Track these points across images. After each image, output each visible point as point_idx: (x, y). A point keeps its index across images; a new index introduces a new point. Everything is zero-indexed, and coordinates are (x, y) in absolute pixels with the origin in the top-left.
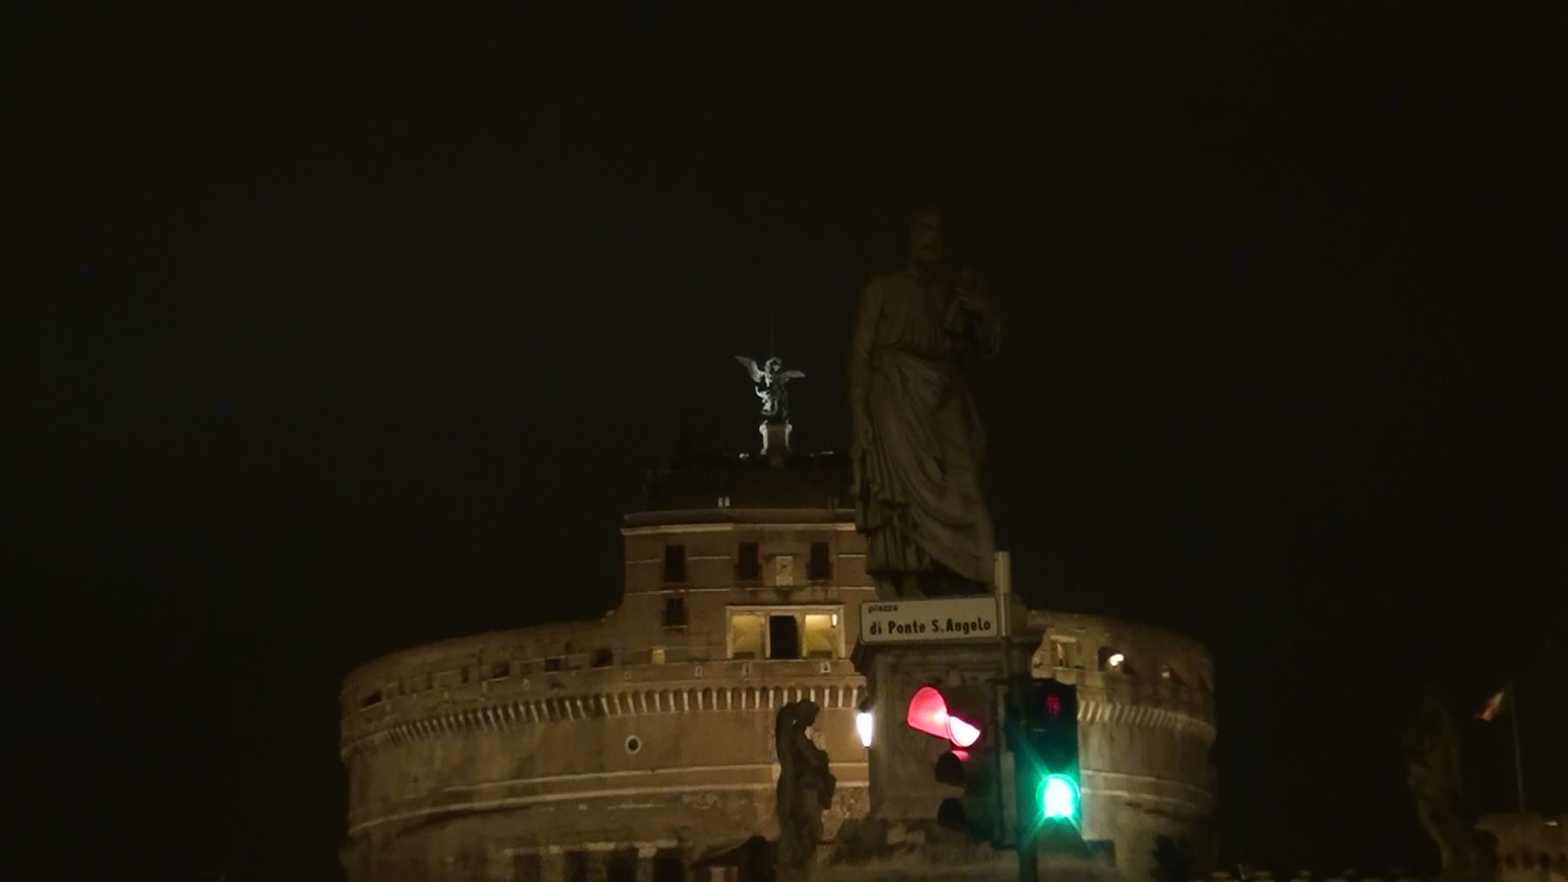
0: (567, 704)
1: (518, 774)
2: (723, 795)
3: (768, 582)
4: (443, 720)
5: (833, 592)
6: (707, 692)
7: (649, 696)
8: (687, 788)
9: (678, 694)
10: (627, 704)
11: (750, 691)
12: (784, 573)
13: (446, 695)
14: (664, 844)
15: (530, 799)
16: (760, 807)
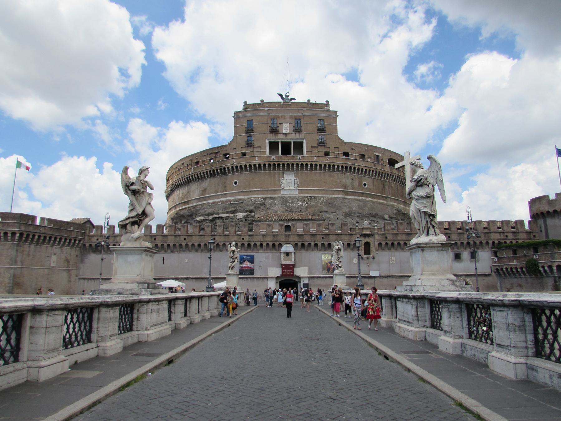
0: (215, 171)
1: (201, 195)
2: (265, 198)
3: (280, 131)
4: (182, 181)
5: (302, 135)
6: (260, 165)
7: (241, 166)
8: (253, 196)
9: (250, 166)
10: (234, 170)
11: (274, 165)
12: (286, 128)
13: (183, 173)
14: (245, 214)
15: (205, 202)
16: (277, 202)
